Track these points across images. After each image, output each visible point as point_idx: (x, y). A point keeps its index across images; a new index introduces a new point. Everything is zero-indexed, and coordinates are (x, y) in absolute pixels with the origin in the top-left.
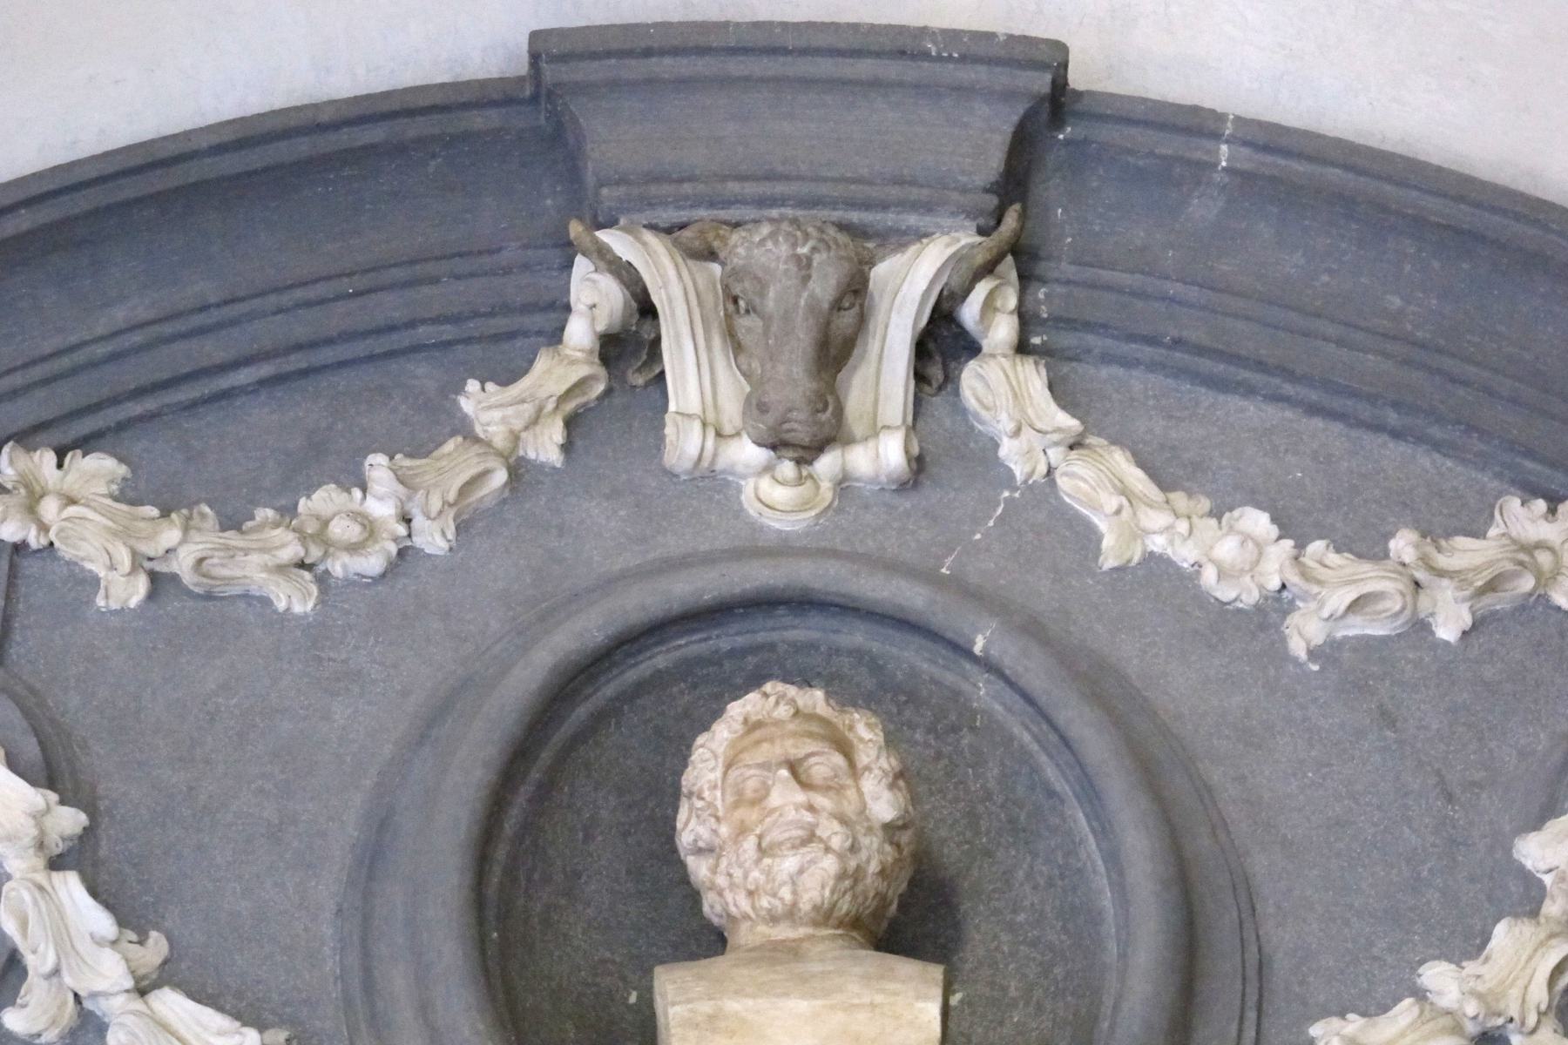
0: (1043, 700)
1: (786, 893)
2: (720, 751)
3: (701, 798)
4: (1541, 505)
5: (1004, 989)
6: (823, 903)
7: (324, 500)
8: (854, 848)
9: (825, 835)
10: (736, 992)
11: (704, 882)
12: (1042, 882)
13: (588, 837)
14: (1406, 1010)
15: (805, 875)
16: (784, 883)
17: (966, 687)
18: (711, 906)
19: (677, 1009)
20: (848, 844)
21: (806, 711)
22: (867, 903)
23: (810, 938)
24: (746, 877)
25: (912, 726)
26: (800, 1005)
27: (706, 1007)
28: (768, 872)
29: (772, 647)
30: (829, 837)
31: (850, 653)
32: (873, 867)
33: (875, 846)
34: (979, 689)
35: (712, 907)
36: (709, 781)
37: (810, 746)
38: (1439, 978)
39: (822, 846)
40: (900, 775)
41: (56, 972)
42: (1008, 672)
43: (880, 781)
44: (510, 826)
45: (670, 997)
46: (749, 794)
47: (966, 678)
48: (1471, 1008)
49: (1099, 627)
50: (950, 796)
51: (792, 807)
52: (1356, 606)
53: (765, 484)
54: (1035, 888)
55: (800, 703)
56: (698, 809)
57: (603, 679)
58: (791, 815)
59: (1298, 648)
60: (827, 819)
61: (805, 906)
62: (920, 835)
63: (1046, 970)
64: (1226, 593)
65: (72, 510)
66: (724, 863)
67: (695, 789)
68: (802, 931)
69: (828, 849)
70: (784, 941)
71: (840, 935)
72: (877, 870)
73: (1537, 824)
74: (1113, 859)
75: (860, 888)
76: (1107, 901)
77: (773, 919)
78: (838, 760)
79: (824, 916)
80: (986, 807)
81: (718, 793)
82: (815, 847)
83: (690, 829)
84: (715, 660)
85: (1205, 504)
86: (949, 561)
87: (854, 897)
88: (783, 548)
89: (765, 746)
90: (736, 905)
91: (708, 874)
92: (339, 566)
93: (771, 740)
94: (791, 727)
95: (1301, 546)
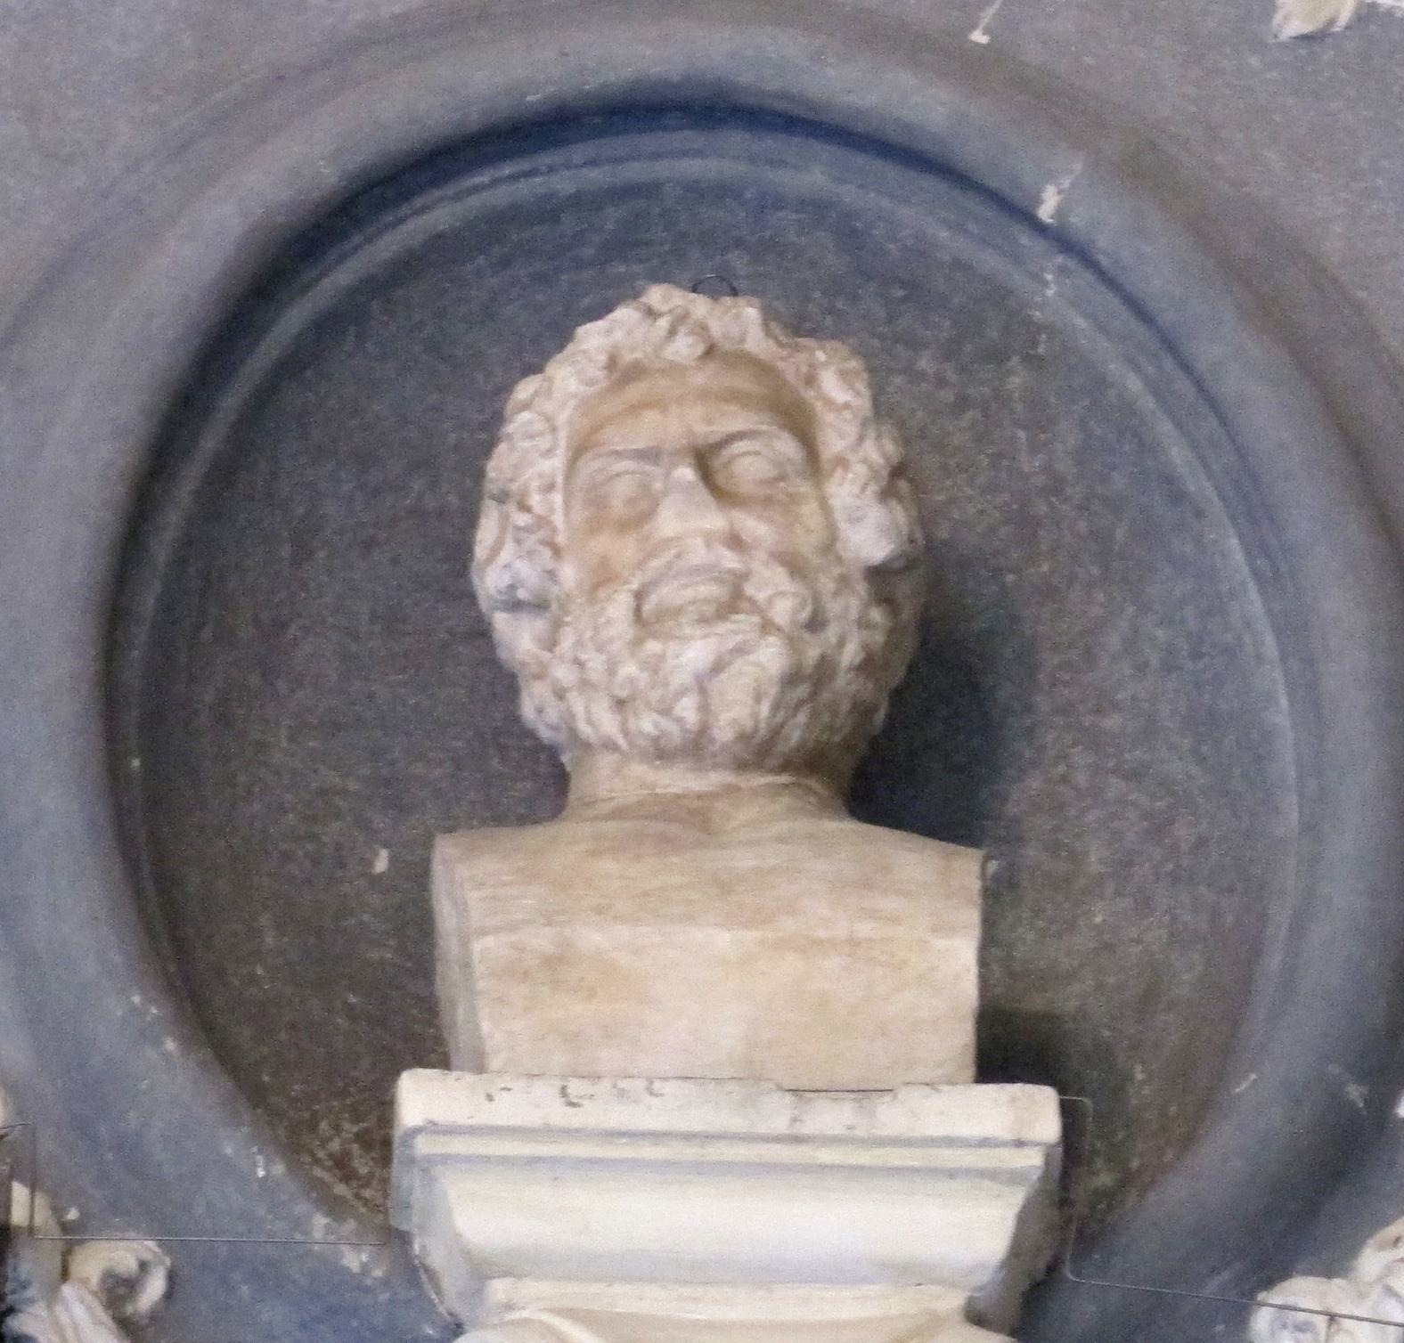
0: (1167, 318)
1: (688, 709)
2: (562, 418)
3: (524, 507)
5: (1076, 858)
6: (756, 730)
8: (815, 623)
9: (761, 597)
10: (599, 910)
11: (524, 664)
12: (1154, 661)
13: (302, 553)
15: (723, 676)
16: (682, 692)
17: (1019, 280)
18: (537, 707)
19: (489, 941)
20: (805, 615)
21: (727, 346)
22: (838, 723)
23: (729, 791)
24: (611, 670)
25: (915, 344)
26: (723, 940)
27: (541, 940)
28: (654, 667)
29: (651, 190)
30: (770, 600)
31: (802, 204)
32: (851, 654)
33: (854, 614)
34: (1046, 284)
35: (540, 711)
36: (541, 476)
37: (737, 420)
39: (756, 619)
40: (898, 471)
42: (1104, 261)
43: (863, 489)
44: (162, 548)
45: (476, 917)
46: (618, 507)
47: (1017, 258)
49: (1272, 156)
50: (981, 480)
51: (699, 541)
54: (1142, 668)
55: (716, 330)
56: (518, 528)
57: (333, 255)
58: (698, 554)
60: (766, 564)
61: (723, 733)
62: (935, 585)
63: (1158, 829)
66: (567, 641)
67: (514, 487)
68: (713, 780)
69: (767, 627)
70: (678, 796)
71: (785, 786)
72: (857, 661)
75: (826, 696)
76: (1281, 714)
77: (661, 753)
78: (787, 446)
80: (1051, 506)
81: (557, 498)
82: (743, 624)
84: (548, 211)
86: (987, 15)
87: (814, 715)
89: (651, 417)
90: (590, 722)
91: (535, 649)
93: (660, 404)
94: (699, 379)
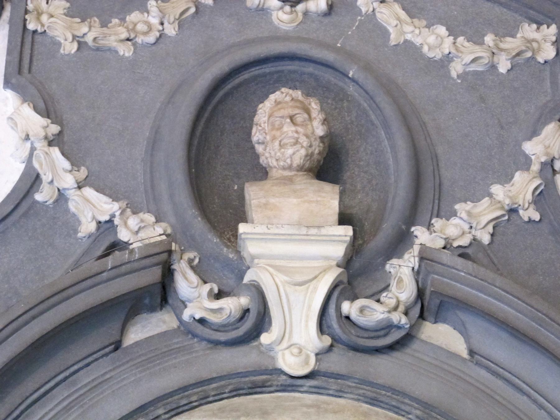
0: (371, 94)
1: (289, 161)
2: (267, 111)
3: (260, 126)
4: (534, 26)
5: (355, 186)
6: (300, 164)
7: (134, 16)
8: (311, 146)
9: (301, 141)
10: (273, 196)
11: (260, 153)
12: (369, 152)
14: (486, 201)
15: (295, 155)
16: (288, 158)
17: (346, 87)
18: (263, 161)
19: (254, 201)
20: (309, 145)
21: (296, 98)
22: (314, 163)
23: (296, 175)
24: (275, 154)
25: (328, 98)
26: (295, 201)
27: (263, 201)
28: (283, 154)
29: (282, 71)
30: (303, 142)
31: (308, 74)
32: (317, 151)
33: (317, 144)
34: (350, 88)
35: (263, 161)
36: (263, 121)
37: (297, 111)
38: (497, 190)
39: (300, 145)
40: (325, 120)
41: (52, 182)
42: (360, 84)
44: (198, 133)
45: (252, 197)
46: (277, 126)
47: (345, 83)
48: (507, 201)
50: (339, 122)
51: (291, 132)
52: (474, 61)
53: (280, 13)
54: (367, 154)
55: (294, 96)
57: (228, 83)
58: (290, 134)
59: (454, 74)
60: (302, 136)
61: (295, 165)
63: (370, 182)
64: (431, 55)
65: (52, 20)
67: (259, 123)
68: (293, 173)
69: (302, 147)
70: (287, 176)
71: (305, 174)
73: (530, 139)
74: (393, 147)
75: (312, 159)
76: (391, 162)
77: (284, 168)
78: (306, 116)
79: (301, 168)
80: (351, 126)
81: (266, 125)
82: (298, 146)
83: (256, 136)
84: (264, 75)
85: (424, 23)
86: (340, 41)
87: (310, 162)
88: (286, 37)
89: (282, 110)
90: (272, 163)
91: (262, 151)
92: (139, 40)
93: (284, 108)
94: (291, 104)
95: (455, 39)
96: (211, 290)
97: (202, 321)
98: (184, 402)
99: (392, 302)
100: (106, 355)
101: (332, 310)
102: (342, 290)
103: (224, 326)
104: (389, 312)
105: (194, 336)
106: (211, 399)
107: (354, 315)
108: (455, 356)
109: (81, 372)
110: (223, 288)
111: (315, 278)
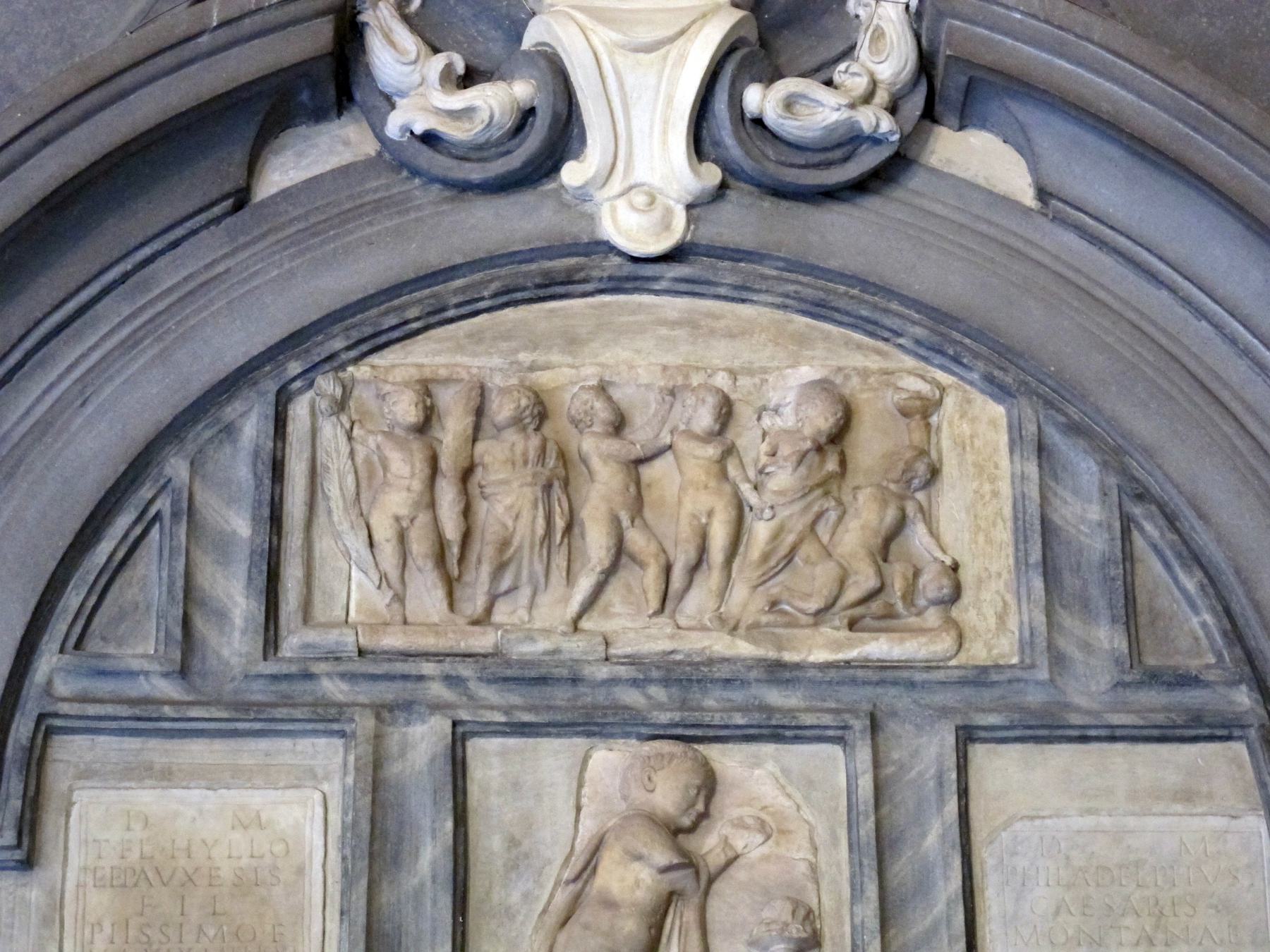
96: (449, 67)
97: (430, 139)
98: (392, 320)
99: (859, 84)
100: (217, 220)
101: (721, 104)
102: (744, 58)
103: (480, 147)
104: (852, 106)
105: (415, 172)
106: (451, 313)
107: (772, 116)
108: (1008, 203)
109: (161, 262)
110: (475, 62)
111: (682, 33)
